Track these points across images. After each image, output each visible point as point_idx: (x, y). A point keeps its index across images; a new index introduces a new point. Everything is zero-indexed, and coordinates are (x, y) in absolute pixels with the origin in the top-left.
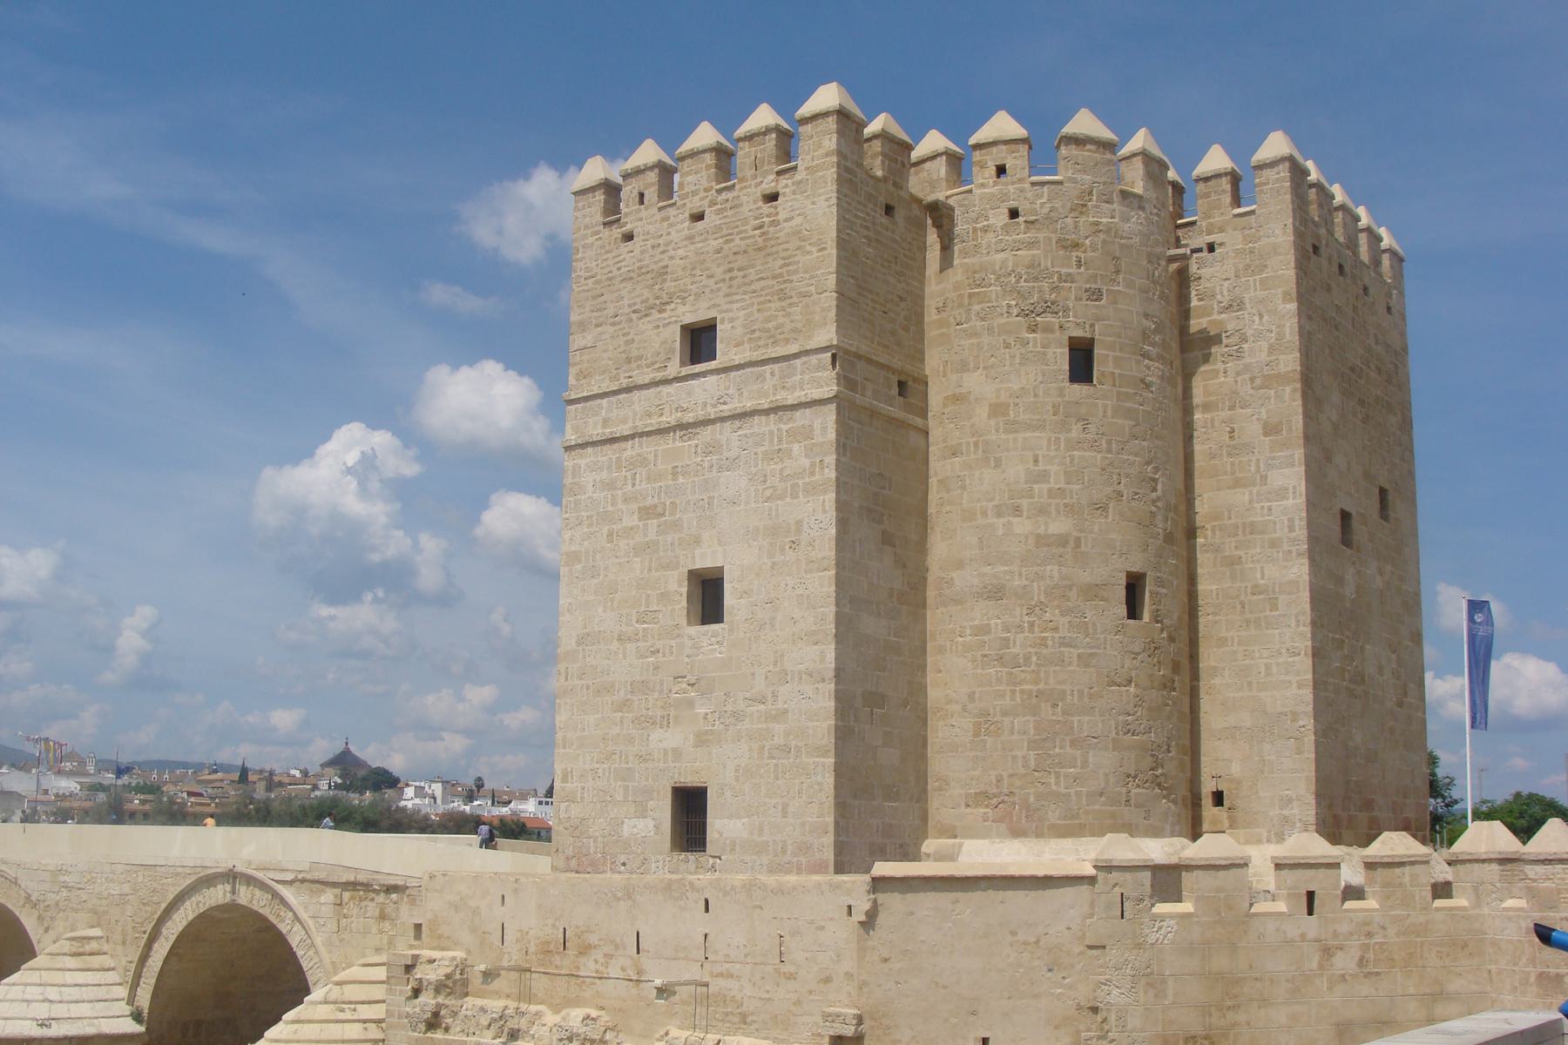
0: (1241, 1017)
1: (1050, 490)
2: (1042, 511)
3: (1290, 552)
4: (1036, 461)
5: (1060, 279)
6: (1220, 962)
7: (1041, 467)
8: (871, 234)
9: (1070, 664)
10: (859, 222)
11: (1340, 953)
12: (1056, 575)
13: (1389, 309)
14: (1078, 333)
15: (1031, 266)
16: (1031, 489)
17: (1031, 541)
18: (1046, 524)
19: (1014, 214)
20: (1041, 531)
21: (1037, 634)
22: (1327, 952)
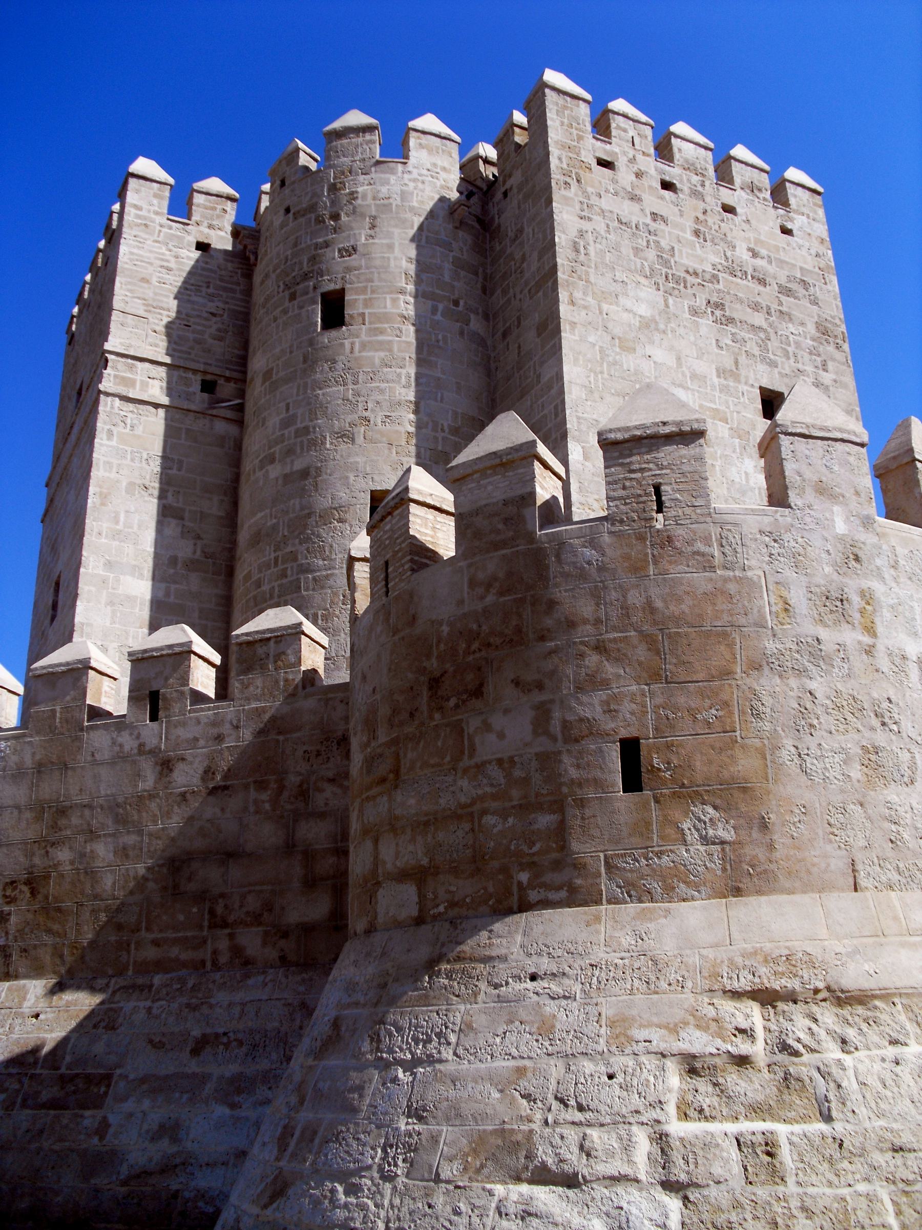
0: (63, 855)
1: (297, 431)
2: (290, 452)
3: (556, 439)
4: (288, 410)
5: (316, 249)
6: (49, 788)
7: (291, 413)
8: (172, 265)
9: (307, 589)
10: (152, 255)
11: (181, 766)
12: (298, 507)
13: (786, 231)
14: (332, 287)
15: (295, 245)
16: (283, 435)
17: (280, 482)
18: (292, 462)
19: (288, 210)
20: (287, 470)
21: (280, 567)
22: (166, 766)
